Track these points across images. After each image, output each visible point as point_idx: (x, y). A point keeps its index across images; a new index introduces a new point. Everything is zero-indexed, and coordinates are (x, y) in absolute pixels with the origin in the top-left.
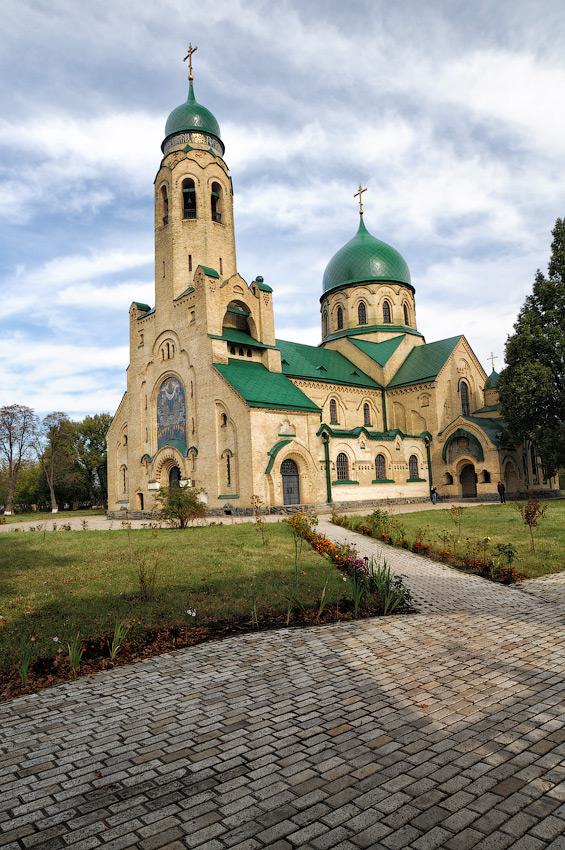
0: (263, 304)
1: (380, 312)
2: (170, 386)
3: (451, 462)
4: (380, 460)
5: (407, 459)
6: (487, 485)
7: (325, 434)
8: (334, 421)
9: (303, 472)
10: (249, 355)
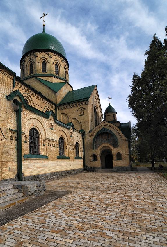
1: (54, 67)
3: (97, 148)
5: (75, 143)
6: (119, 162)
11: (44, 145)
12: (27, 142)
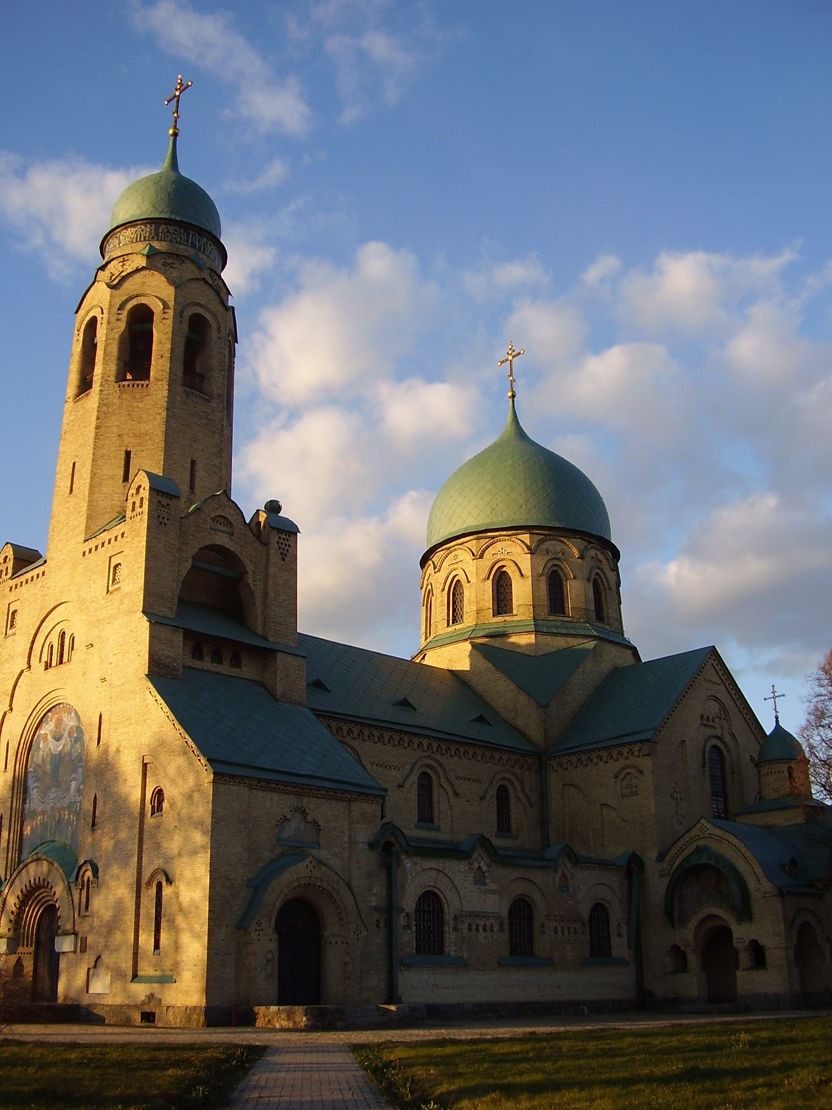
0: (275, 557)
2: (59, 722)
4: (521, 912)
5: (585, 911)
6: (758, 976)
7: (389, 848)
8: (426, 815)
9: (332, 928)
10: (236, 662)
11: (456, 929)
12: (411, 929)
